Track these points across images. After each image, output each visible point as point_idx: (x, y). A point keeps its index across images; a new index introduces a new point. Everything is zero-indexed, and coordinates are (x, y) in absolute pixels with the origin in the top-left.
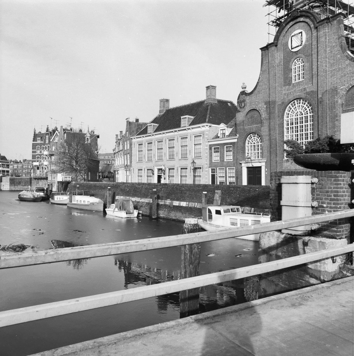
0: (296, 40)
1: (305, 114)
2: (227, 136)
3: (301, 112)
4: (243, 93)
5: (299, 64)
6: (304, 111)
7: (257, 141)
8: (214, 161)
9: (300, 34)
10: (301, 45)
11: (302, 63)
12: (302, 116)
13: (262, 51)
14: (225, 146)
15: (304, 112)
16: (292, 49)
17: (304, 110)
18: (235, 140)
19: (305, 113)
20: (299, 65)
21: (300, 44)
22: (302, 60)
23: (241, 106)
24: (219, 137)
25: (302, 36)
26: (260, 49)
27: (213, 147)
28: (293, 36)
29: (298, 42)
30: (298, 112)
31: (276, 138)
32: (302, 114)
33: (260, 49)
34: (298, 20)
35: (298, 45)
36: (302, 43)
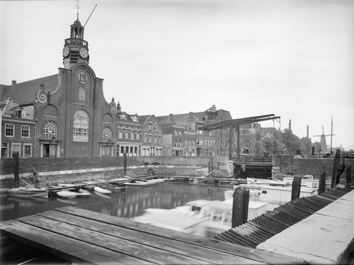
25: (86, 77)
26: (59, 68)
33: (59, 68)
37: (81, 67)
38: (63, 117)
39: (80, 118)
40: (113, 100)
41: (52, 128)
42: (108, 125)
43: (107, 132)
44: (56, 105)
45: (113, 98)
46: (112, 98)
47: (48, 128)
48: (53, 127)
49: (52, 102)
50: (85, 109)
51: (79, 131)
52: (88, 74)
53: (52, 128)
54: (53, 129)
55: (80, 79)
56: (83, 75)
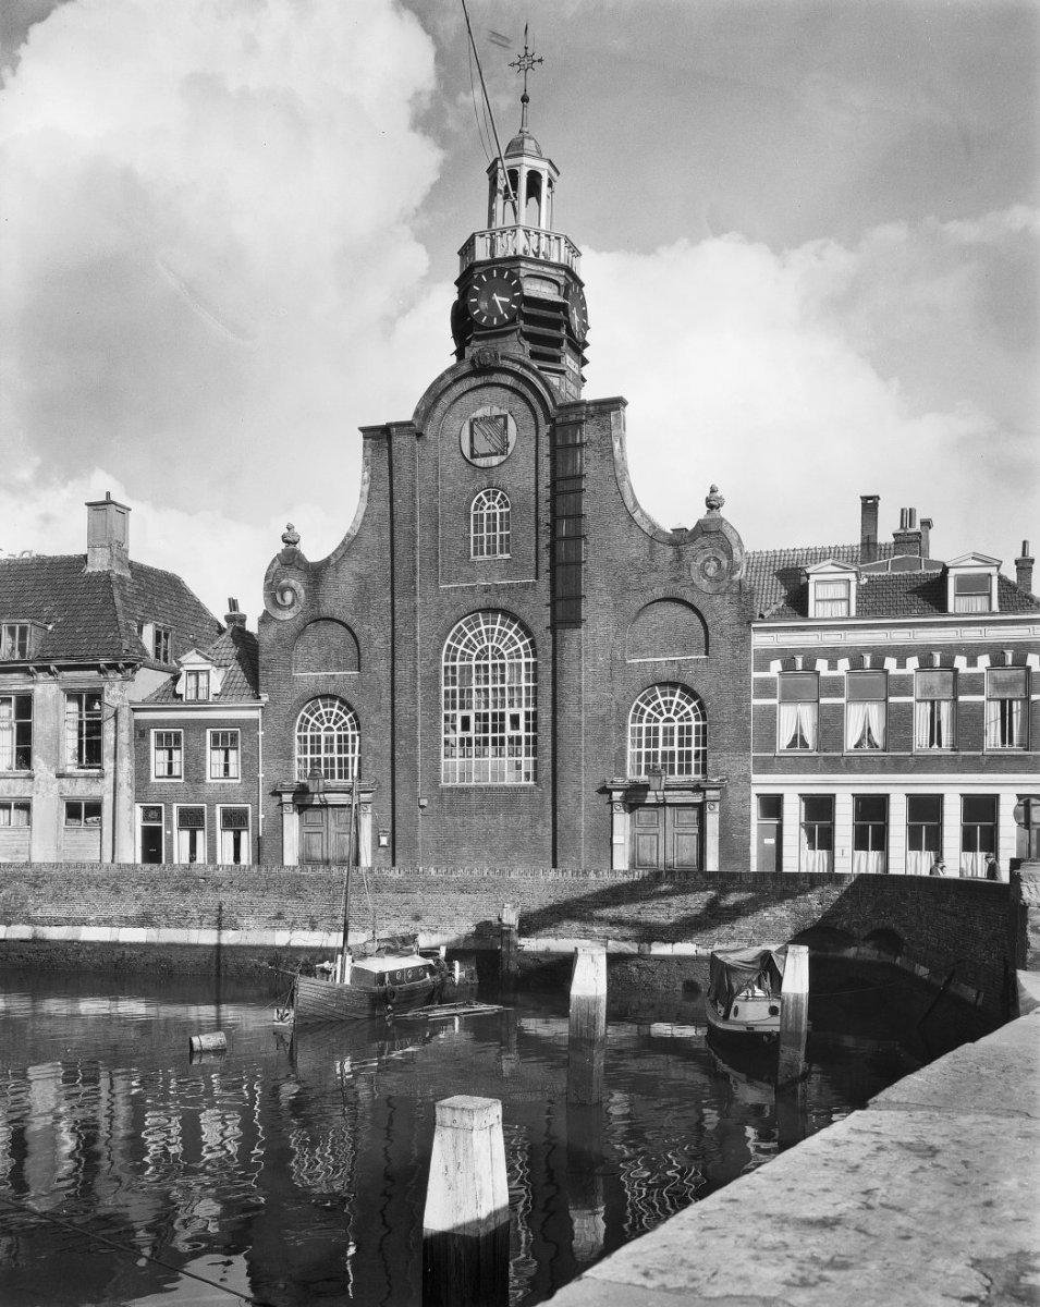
3: (498, 650)
4: (290, 558)
5: (494, 507)
7: (340, 724)
9: (501, 420)
11: (501, 507)
13: (365, 437)
14: (208, 731)
15: (509, 651)
16: (473, 456)
19: (511, 653)
20: (492, 511)
22: (502, 496)
23: (279, 600)
25: (506, 427)
26: (362, 429)
27: (152, 731)
30: (487, 647)
31: (416, 719)
32: (502, 656)
33: (362, 429)
34: (496, 378)
37: (474, 381)
38: (382, 668)
39: (478, 658)
40: (712, 505)
41: (335, 728)
42: (667, 674)
43: (669, 720)
44: (347, 618)
45: (713, 491)
46: (707, 494)
47: (319, 729)
48: (345, 724)
49: (329, 606)
50: (502, 602)
51: (527, 730)
52: (520, 406)
53: (335, 728)
54: (342, 733)
55: (472, 449)
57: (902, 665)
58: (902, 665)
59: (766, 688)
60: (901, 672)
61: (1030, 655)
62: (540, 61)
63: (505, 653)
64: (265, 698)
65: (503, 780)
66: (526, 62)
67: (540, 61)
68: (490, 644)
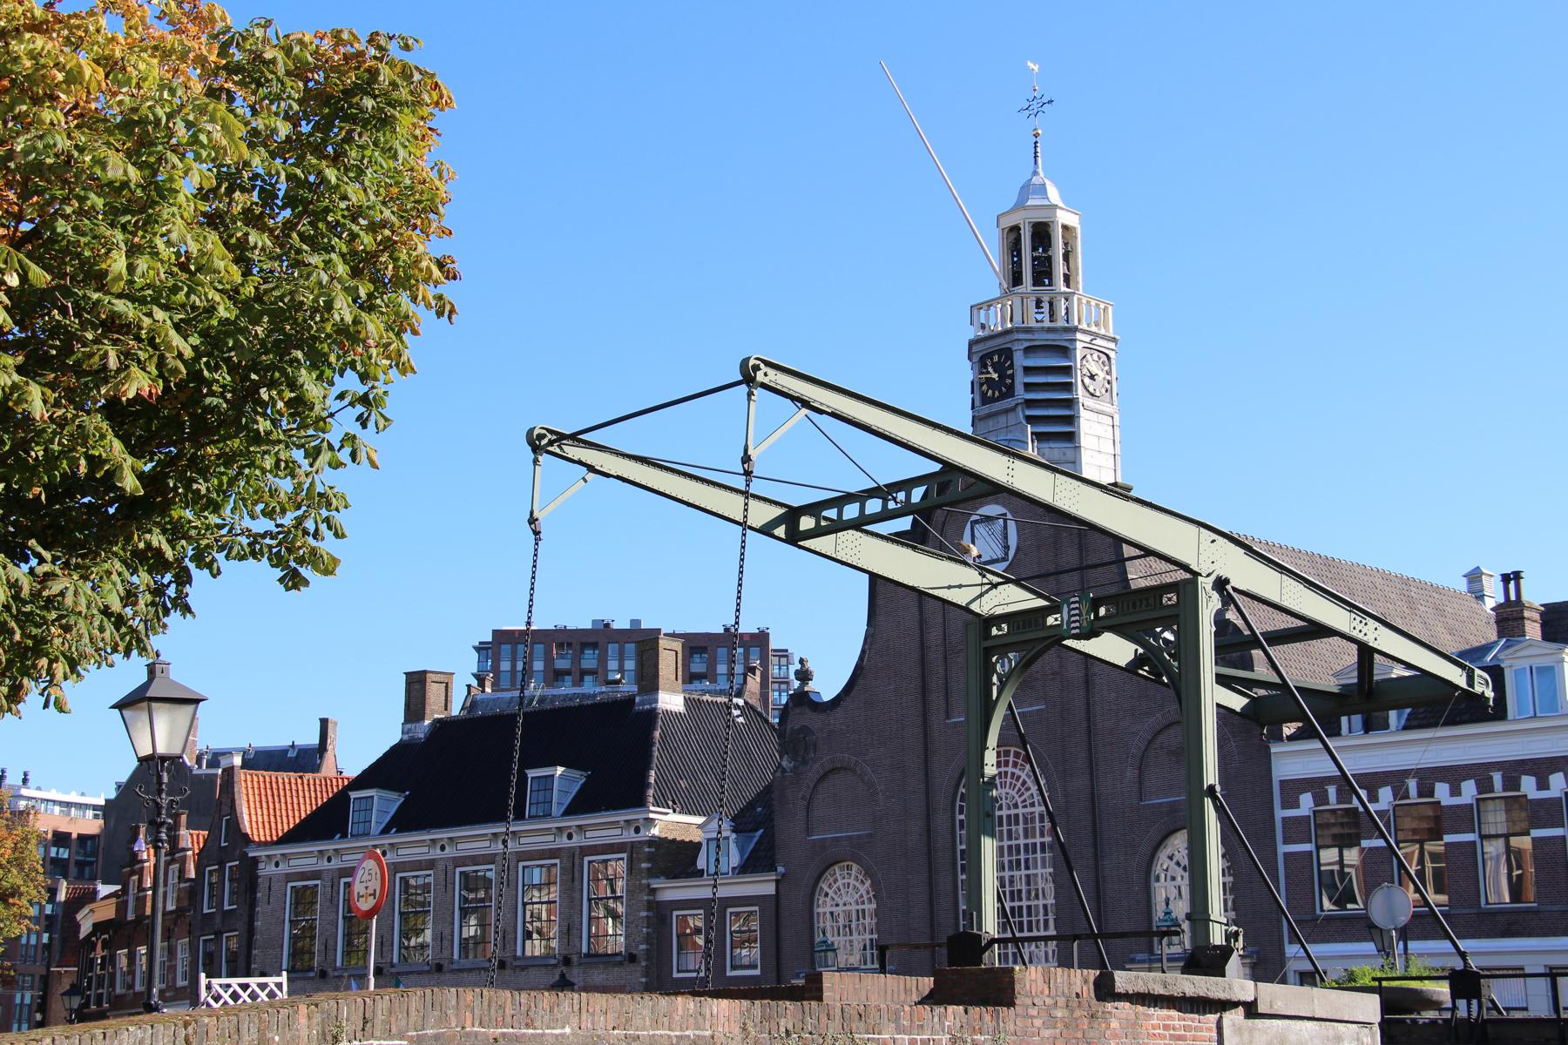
0: (988, 539)
1: (1025, 807)
2: (734, 869)
6: (1023, 794)
8: (678, 971)
9: (1001, 521)
10: (1004, 559)
12: (1016, 811)
15: (1023, 798)
17: (1023, 789)
18: (770, 889)
21: (1000, 554)
24: (700, 873)
28: (976, 522)
29: (994, 546)
32: (1016, 806)
35: (995, 557)
36: (1007, 554)
56: (988, 519)
57: (1456, 791)
58: (1456, 791)
59: (1296, 829)
60: (1456, 801)
61: (1561, 774)
62: (1050, 102)
63: (1019, 800)
64: (781, 869)
65: (1008, 963)
66: (1035, 106)
67: (1050, 102)
68: (1003, 791)
